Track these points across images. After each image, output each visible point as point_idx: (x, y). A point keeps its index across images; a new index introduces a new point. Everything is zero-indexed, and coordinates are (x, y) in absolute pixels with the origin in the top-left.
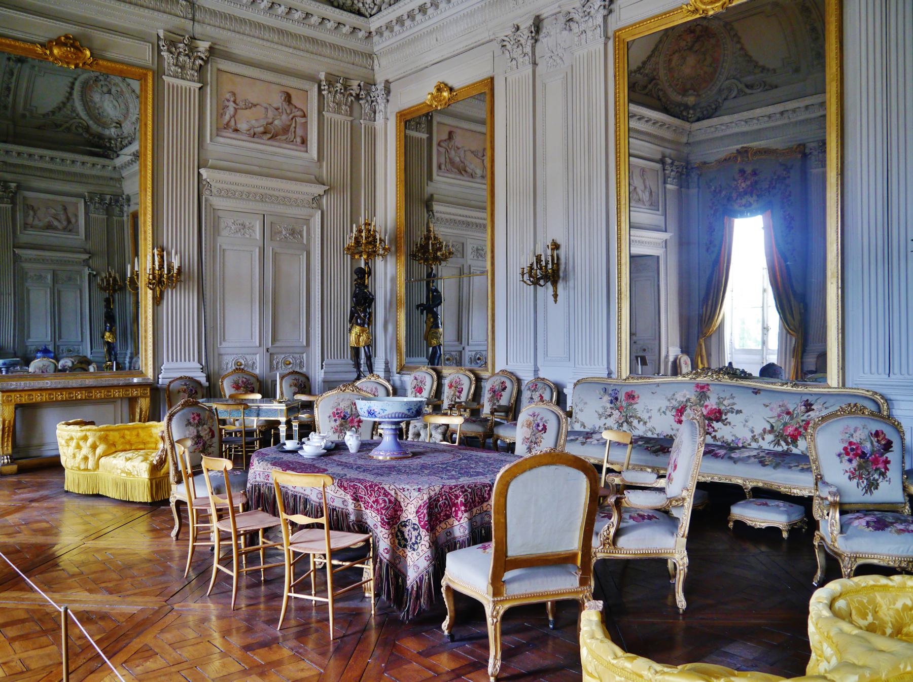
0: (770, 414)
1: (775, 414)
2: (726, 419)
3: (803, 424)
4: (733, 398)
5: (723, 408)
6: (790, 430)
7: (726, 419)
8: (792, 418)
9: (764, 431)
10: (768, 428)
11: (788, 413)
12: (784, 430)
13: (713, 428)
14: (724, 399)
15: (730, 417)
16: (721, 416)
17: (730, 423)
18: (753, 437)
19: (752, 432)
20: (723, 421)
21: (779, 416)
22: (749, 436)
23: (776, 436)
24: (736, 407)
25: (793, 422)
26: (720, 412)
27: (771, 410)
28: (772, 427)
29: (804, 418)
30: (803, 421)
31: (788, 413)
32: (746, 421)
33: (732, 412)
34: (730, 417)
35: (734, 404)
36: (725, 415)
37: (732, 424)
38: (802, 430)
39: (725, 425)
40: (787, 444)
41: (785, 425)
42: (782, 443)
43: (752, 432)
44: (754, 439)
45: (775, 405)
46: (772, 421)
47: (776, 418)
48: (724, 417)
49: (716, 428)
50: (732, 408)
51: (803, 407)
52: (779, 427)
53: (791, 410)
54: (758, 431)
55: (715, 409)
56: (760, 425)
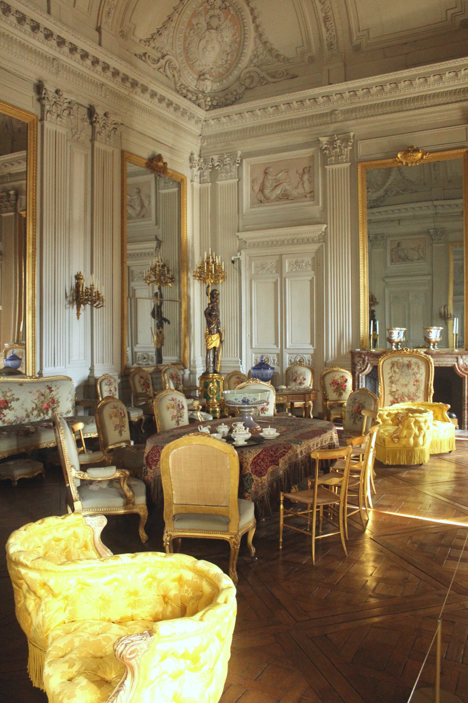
0: (34, 397)
1: (37, 397)
2: (11, 406)
3: (50, 400)
4: (11, 390)
5: (8, 398)
6: (45, 405)
7: (11, 406)
8: (45, 398)
9: (33, 409)
10: (35, 406)
11: (43, 395)
12: (42, 406)
13: (3, 414)
14: (6, 393)
15: (13, 404)
16: (8, 405)
17: (13, 408)
18: (27, 414)
19: (26, 411)
20: (9, 408)
21: (39, 397)
22: (24, 414)
23: (39, 411)
24: (16, 397)
25: (46, 400)
26: (6, 402)
27: (34, 394)
28: (36, 405)
29: (50, 396)
30: (50, 398)
31: (43, 395)
32: (23, 405)
33: (14, 400)
34: (13, 404)
35: (13, 395)
36: (10, 403)
37: (15, 409)
38: (50, 404)
39: (11, 410)
40: (44, 414)
41: (42, 402)
42: (42, 414)
43: (26, 411)
44: (28, 416)
45: (34, 391)
46: (36, 401)
47: (38, 400)
48: (10, 405)
49: (5, 414)
50: (13, 398)
51: (48, 390)
52: (39, 405)
53: (43, 393)
54: (30, 410)
55: (3, 400)
56: (30, 406)
